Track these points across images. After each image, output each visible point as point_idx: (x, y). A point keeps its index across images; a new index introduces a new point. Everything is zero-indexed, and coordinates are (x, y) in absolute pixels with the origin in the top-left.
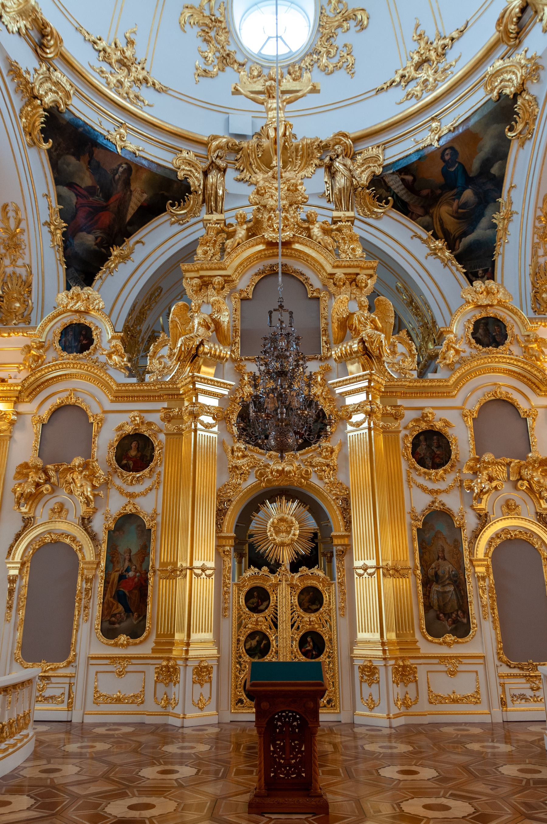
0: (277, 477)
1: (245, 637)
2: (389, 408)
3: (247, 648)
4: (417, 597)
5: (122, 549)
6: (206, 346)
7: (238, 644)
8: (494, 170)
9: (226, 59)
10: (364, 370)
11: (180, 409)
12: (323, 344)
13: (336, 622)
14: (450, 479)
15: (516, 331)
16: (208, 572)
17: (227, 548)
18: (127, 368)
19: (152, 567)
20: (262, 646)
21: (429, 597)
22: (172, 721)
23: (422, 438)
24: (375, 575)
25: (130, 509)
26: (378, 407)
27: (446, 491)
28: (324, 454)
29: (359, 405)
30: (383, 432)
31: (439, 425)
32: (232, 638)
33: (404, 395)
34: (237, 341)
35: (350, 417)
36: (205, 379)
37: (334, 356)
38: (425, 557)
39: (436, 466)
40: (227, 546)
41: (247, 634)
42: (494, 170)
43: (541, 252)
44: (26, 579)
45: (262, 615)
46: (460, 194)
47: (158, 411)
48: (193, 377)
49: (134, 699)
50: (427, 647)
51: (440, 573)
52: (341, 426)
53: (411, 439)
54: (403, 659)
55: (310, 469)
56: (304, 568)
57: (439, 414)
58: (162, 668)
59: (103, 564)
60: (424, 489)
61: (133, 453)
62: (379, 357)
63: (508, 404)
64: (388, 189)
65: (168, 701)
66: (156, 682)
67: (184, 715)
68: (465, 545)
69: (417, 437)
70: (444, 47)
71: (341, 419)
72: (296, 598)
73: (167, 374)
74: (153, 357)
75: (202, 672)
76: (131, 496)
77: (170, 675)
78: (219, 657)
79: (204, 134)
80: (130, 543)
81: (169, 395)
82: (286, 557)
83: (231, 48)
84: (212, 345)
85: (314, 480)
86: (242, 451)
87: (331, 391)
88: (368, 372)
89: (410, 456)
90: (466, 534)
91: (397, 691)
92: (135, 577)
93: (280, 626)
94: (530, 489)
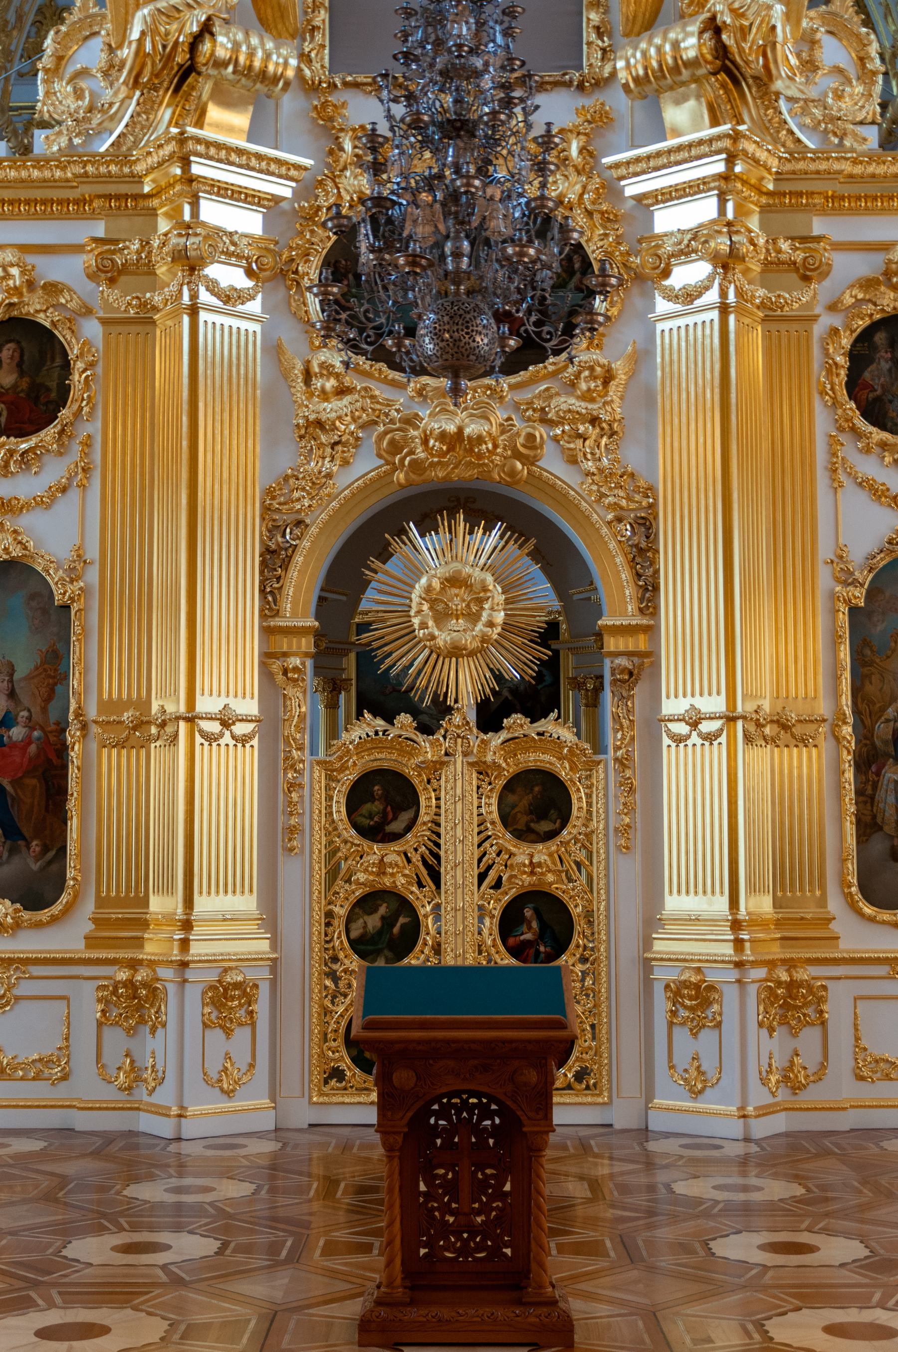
0: (442, 454)
1: (347, 906)
2: (785, 246)
3: (354, 934)
4: (840, 798)
6: (221, 39)
7: (328, 924)
10: (715, 122)
11: (146, 244)
12: (589, 35)
13: (607, 868)
16: (241, 729)
17: (295, 661)
19: (78, 715)
20: (396, 930)
21: (872, 798)
22: (147, 1123)
23: (880, 338)
24: (723, 739)
26: (752, 242)
28: (584, 386)
29: (695, 234)
30: (766, 320)
32: (311, 909)
33: (835, 204)
34: (317, 22)
35: (666, 273)
36: (219, 146)
37: (623, 76)
38: (870, 689)
40: (295, 654)
41: (353, 899)
45: (396, 847)
47: (77, 249)
48: (182, 139)
49: (40, 1069)
52: (638, 301)
53: (846, 342)
54: (790, 964)
55: (541, 431)
56: (517, 718)
58: (116, 988)
62: (763, 81)
65: (136, 1074)
66: (100, 1024)
67: (182, 1108)
69: (865, 337)
71: (639, 277)
72: (494, 801)
73: (102, 131)
74: (55, 72)
75: (228, 998)
77: (139, 1007)
78: (274, 960)
81: (109, 197)
82: (467, 686)
84: (240, 36)
85: (552, 464)
86: (337, 376)
87: (610, 190)
88: (725, 128)
89: (843, 394)
91: (771, 1047)
92: (28, 741)
93: (446, 879)
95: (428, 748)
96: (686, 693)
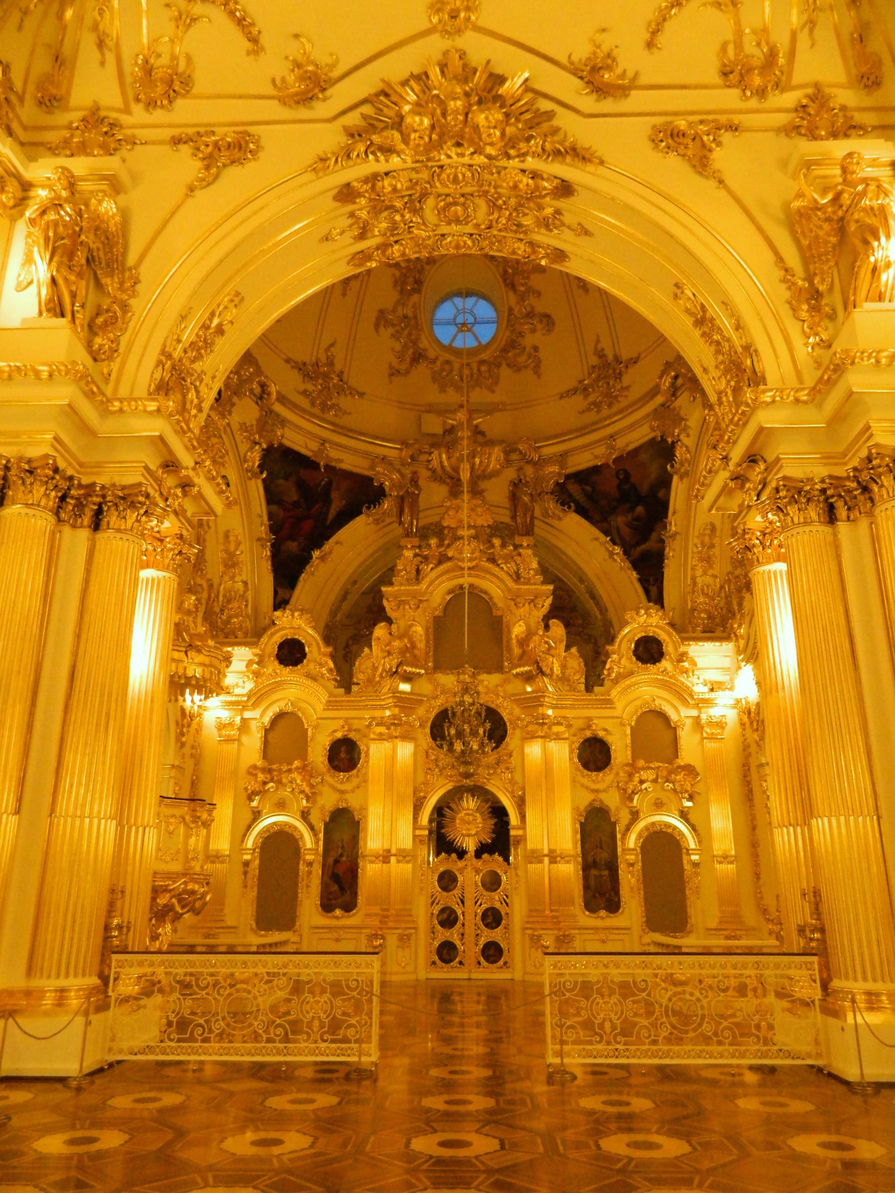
9: (418, 357)
18: (335, 680)
25: (342, 805)
27: (605, 791)
31: (601, 734)
38: (587, 846)
43: (699, 572)
44: (257, 862)
46: (632, 509)
50: (586, 919)
51: (597, 860)
57: (603, 723)
59: (321, 849)
63: (662, 716)
68: (619, 836)
76: (342, 792)
80: (342, 835)
82: (470, 845)
95: (461, 864)
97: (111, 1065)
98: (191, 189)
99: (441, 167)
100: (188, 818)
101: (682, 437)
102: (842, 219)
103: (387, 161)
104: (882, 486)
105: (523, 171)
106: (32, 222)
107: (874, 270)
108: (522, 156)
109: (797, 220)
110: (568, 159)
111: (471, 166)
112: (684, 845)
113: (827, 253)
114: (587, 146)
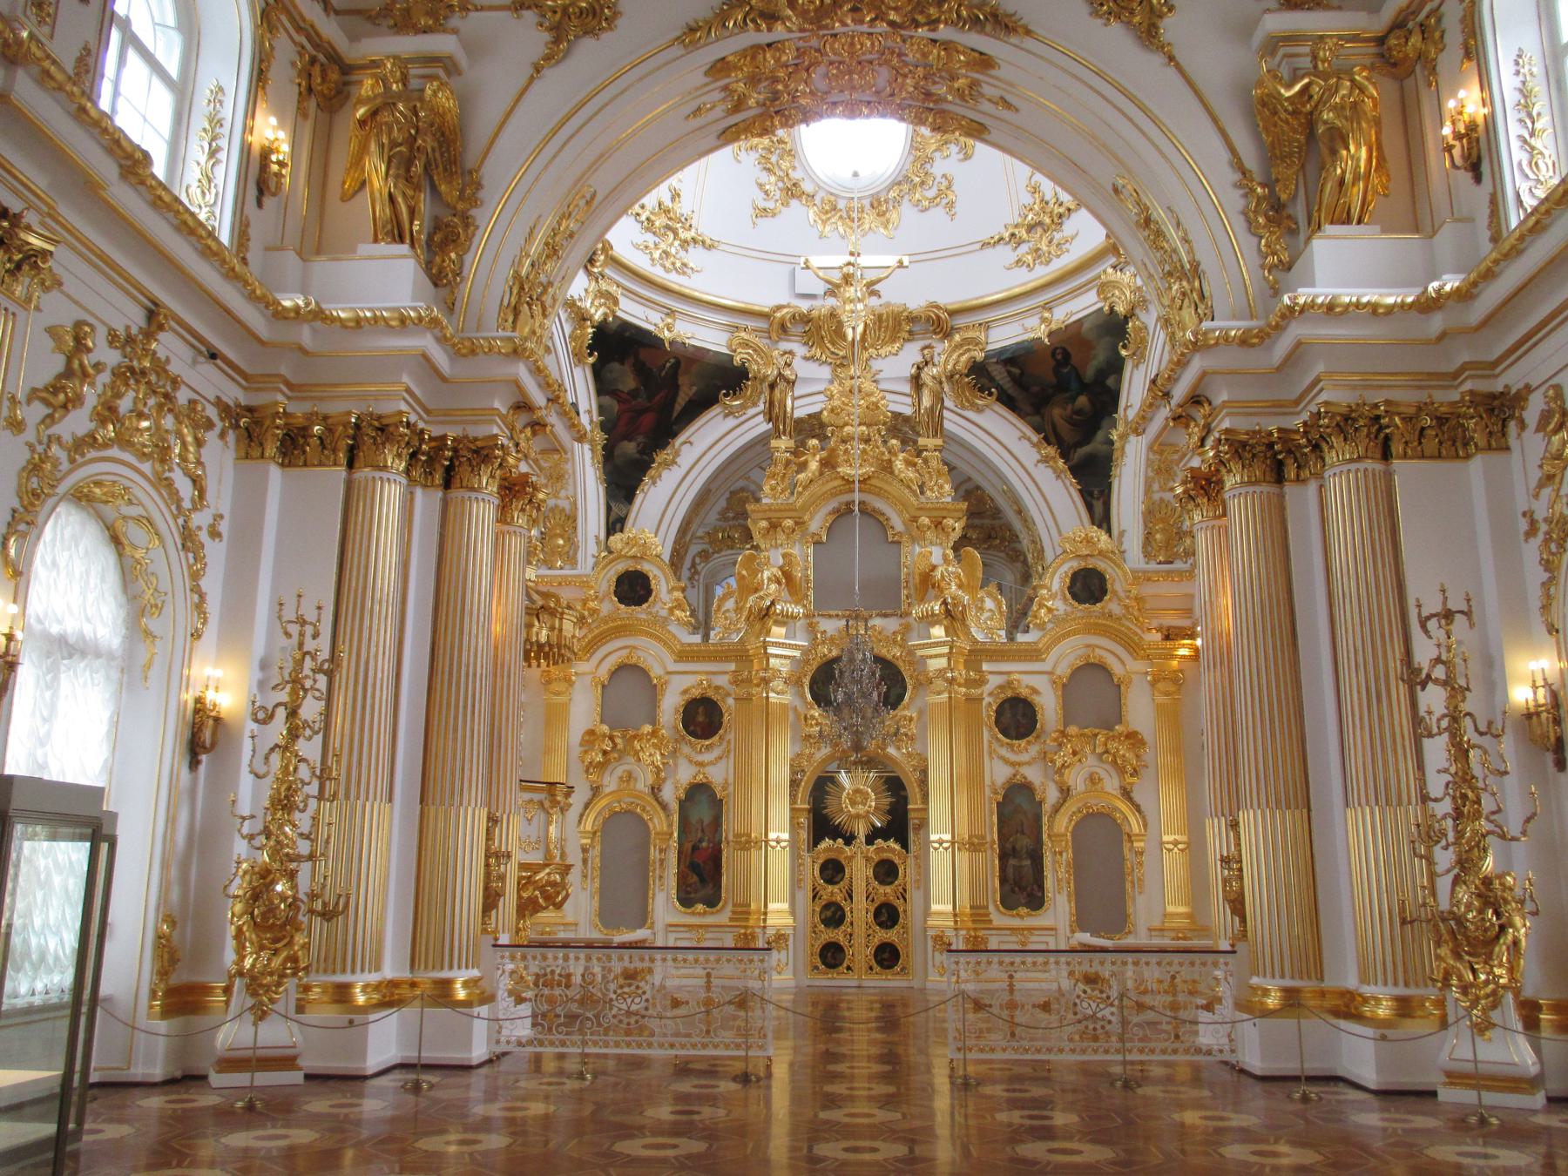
5: (694, 817)
8: (1110, 382)
9: (793, 191)
14: (1034, 750)
15: (1118, 587)
27: (1028, 763)
31: (1024, 692)
39: (1020, 736)
42: (1110, 382)
43: (1156, 487)
44: (598, 848)
46: (1073, 399)
50: (999, 918)
57: (1027, 680)
60: (1006, 761)
61: (700, 718)
62: (964, 620)
64: (992, 379)
68: (1045, 819)
69: (1001, 706)
70: (1061, 216)
76: (701, 764)
79: (764, 302)
80: (702, 813)
82: (861, 831)
83: (796, 175)
87: (911, 652)
90: (1047, 808)
94: (1114, 762)
96: (939, 833)
97: (498, 1057)
98: (538, 69)
99: (835, 35)
100: (547, 804)
101: (1137, 311)
102: (1311, 113)
103: (769, 30)
104: (1332, 447)
105: (934, 41)
106: (362, 123)
107: (1342, 182)
108: (933, 23)
109: (1263, 110)
110: (988, 28)
111: (870, 34)
112: (1127, 829)
113: (1290, 155)
114: (1010, 10)
